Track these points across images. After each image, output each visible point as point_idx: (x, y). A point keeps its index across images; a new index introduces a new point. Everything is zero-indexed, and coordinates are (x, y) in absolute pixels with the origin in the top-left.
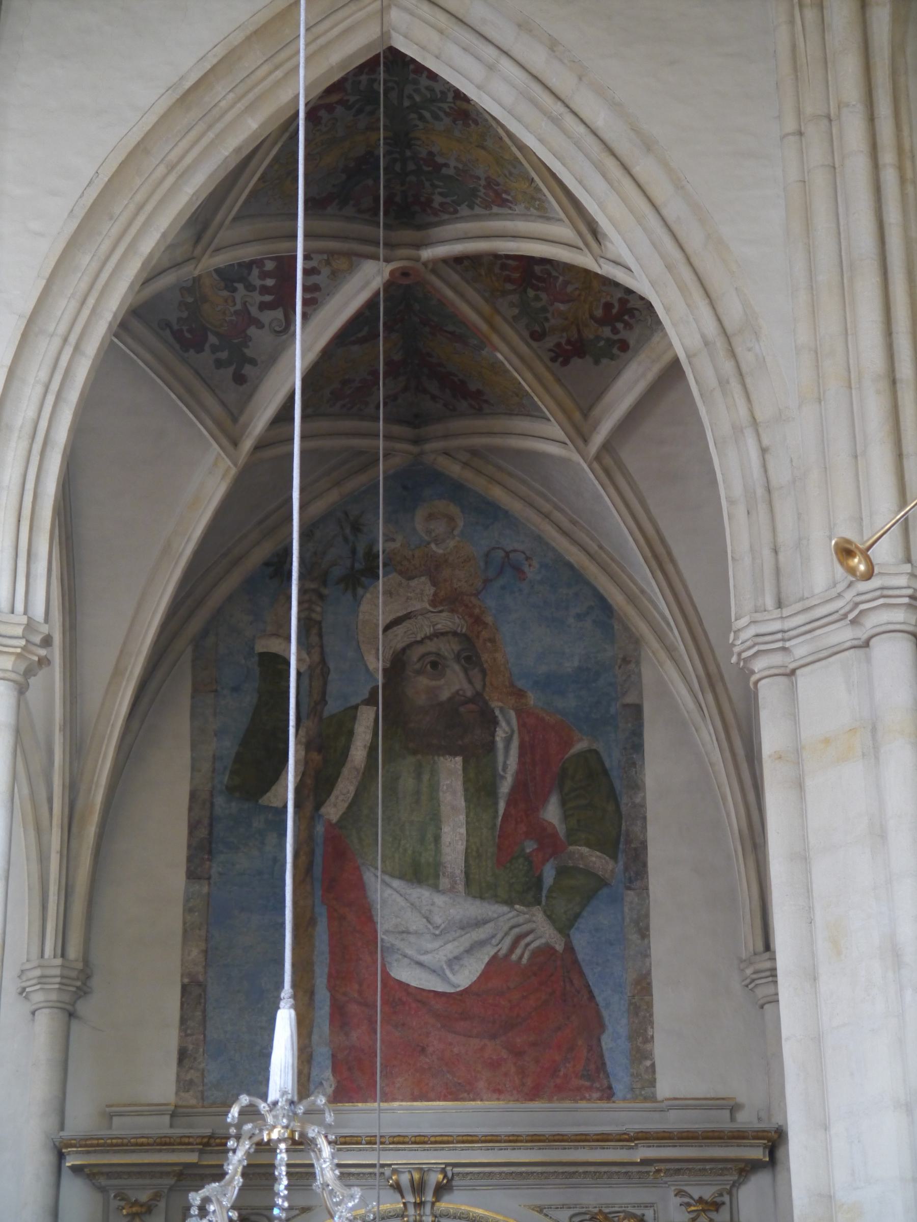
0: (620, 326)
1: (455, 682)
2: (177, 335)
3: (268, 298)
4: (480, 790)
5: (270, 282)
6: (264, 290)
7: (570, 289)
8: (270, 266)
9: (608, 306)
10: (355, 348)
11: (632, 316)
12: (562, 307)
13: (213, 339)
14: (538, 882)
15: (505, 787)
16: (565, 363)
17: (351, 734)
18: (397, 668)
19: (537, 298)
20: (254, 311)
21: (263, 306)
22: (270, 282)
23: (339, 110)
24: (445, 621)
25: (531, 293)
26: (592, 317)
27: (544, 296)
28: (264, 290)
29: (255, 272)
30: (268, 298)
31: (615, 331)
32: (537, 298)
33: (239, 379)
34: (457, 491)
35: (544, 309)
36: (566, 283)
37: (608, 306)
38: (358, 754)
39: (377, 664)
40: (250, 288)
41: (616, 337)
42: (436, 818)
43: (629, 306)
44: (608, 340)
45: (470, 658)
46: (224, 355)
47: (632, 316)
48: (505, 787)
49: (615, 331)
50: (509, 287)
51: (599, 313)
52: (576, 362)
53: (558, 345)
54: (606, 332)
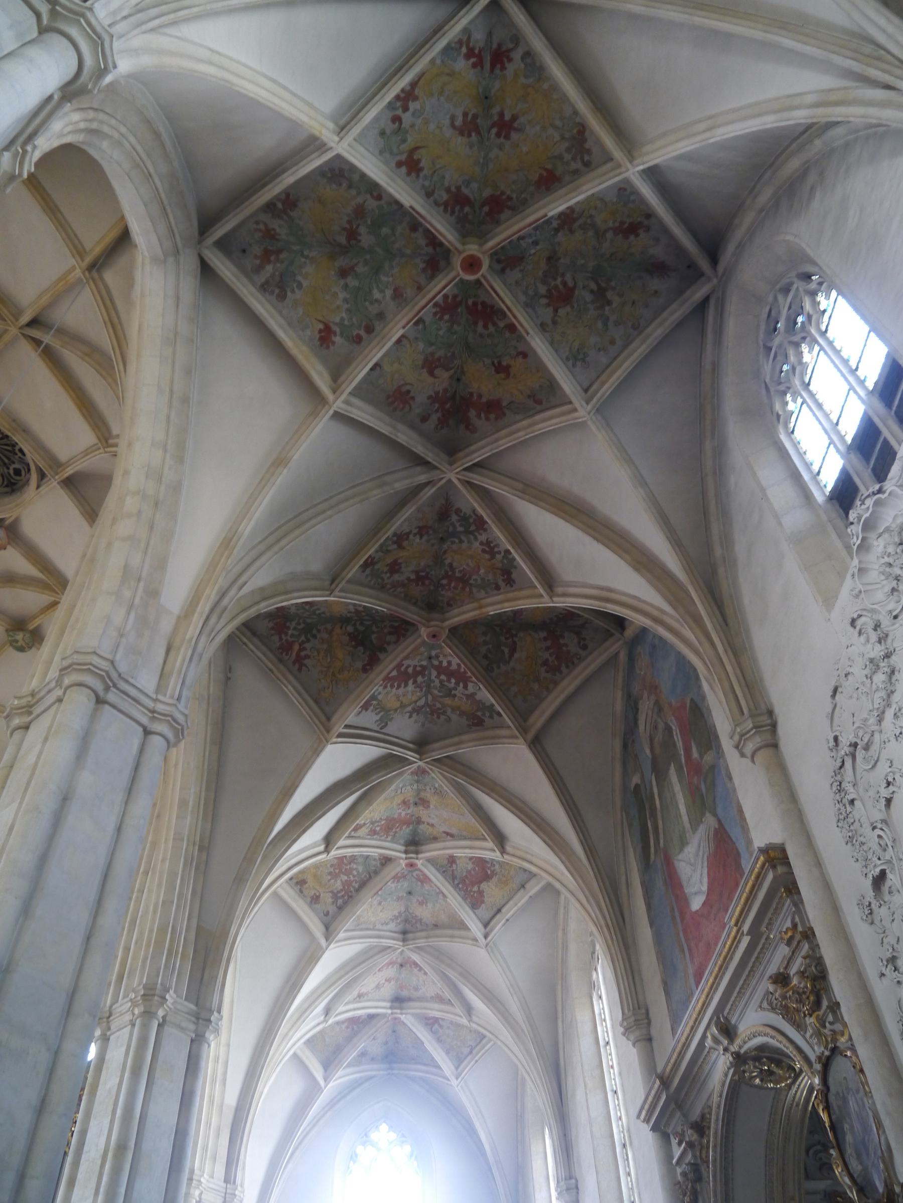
0: (496, 550)
3: (461, 685)
5: (453, 681)
6: (457, 684)
7: (471, 564)
8: (443, 677)
9: (484, 551)
10: (516, 655)
11: (491, 542)
12: (482, 571)
13: (479, 714)
16: (514, 582)
19: (476, 580)
20: (466, 692)
21: (466, 687)
22: (453, 681)
23: (307, 645)
25: (472, 581)
26: (490, 560)
27: (474, 577)
28: (457, 684)
29: (446, 683)
30: (461, 685)
31: (499, 553)
32: (476, 580)
35: (483, 579)
36: (468, 565)
37: (484, 551)
40: (455, 689)
41: (503, 554)
43: (485, 541)
44: (503, 557)
46: (487, 714)
47: (491, 542)
49: (499, 553)
50: (468, 589)
51: (487, 556)
52: (514, 576)
53: (503, 580)
54: (499, 557)
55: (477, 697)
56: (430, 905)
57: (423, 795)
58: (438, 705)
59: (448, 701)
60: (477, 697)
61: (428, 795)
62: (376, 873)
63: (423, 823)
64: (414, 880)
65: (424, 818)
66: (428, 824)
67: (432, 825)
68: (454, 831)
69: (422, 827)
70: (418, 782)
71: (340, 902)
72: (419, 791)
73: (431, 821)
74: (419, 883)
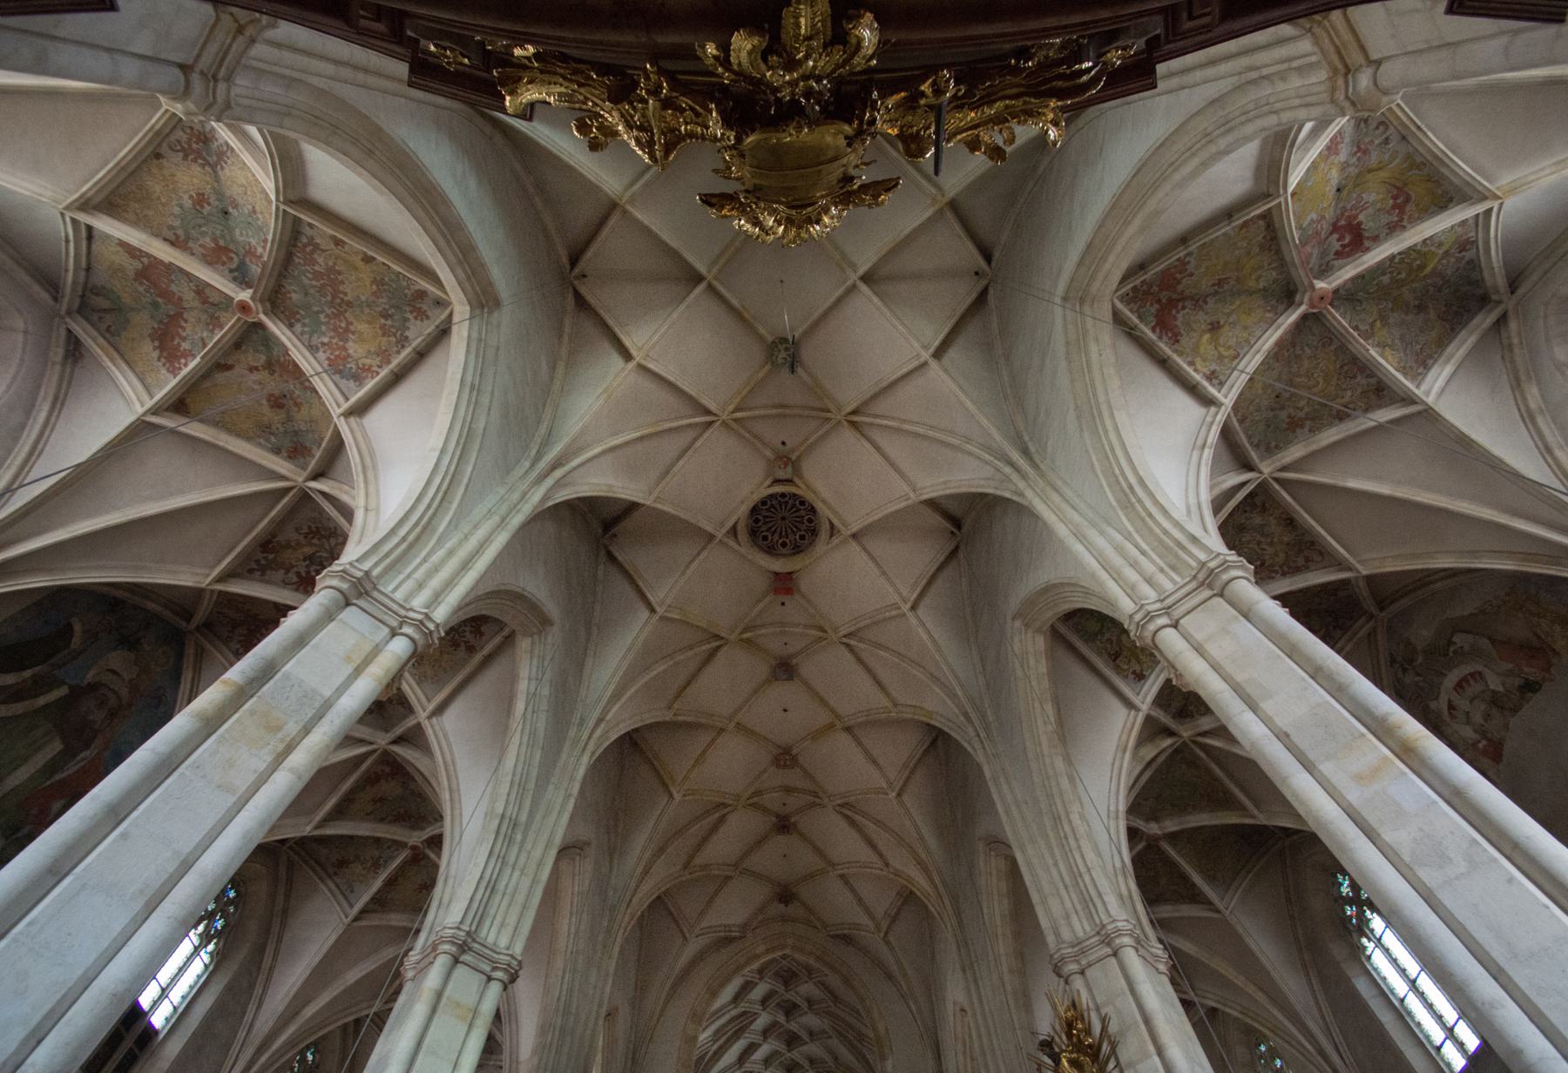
1: (98, 716)
2: (269, 542)
4: (52, 767)
13: (271, 556)
14: (18, 830)
15: (58, 777)
17: (49, 690)
18: (93, 687)
21: (298, 574)
24: (124, 692)
33: (251, 571)
34: (180, 656)
38: (42, 701)
39: (90, 676)
42: (26, 759)
45: (112, 714)
48: (58, 777)
55: (282, 571)
56: (188, 203)
57: (282, 415)
58: (315, 541)
59: (308, 550)
60: (282, 571)
61: (276, 417)
62: (281, 275)
63: (264, 368)
64: (231, 247)
65: (263, 375)
66: (257, 369)
67: (252, 369)
68: (221, 377)
69: (262, 359)
70: (296, 433)
71: (305, 240)
72: (289, 419)
73: (255, 376)
74: (222, 243)
